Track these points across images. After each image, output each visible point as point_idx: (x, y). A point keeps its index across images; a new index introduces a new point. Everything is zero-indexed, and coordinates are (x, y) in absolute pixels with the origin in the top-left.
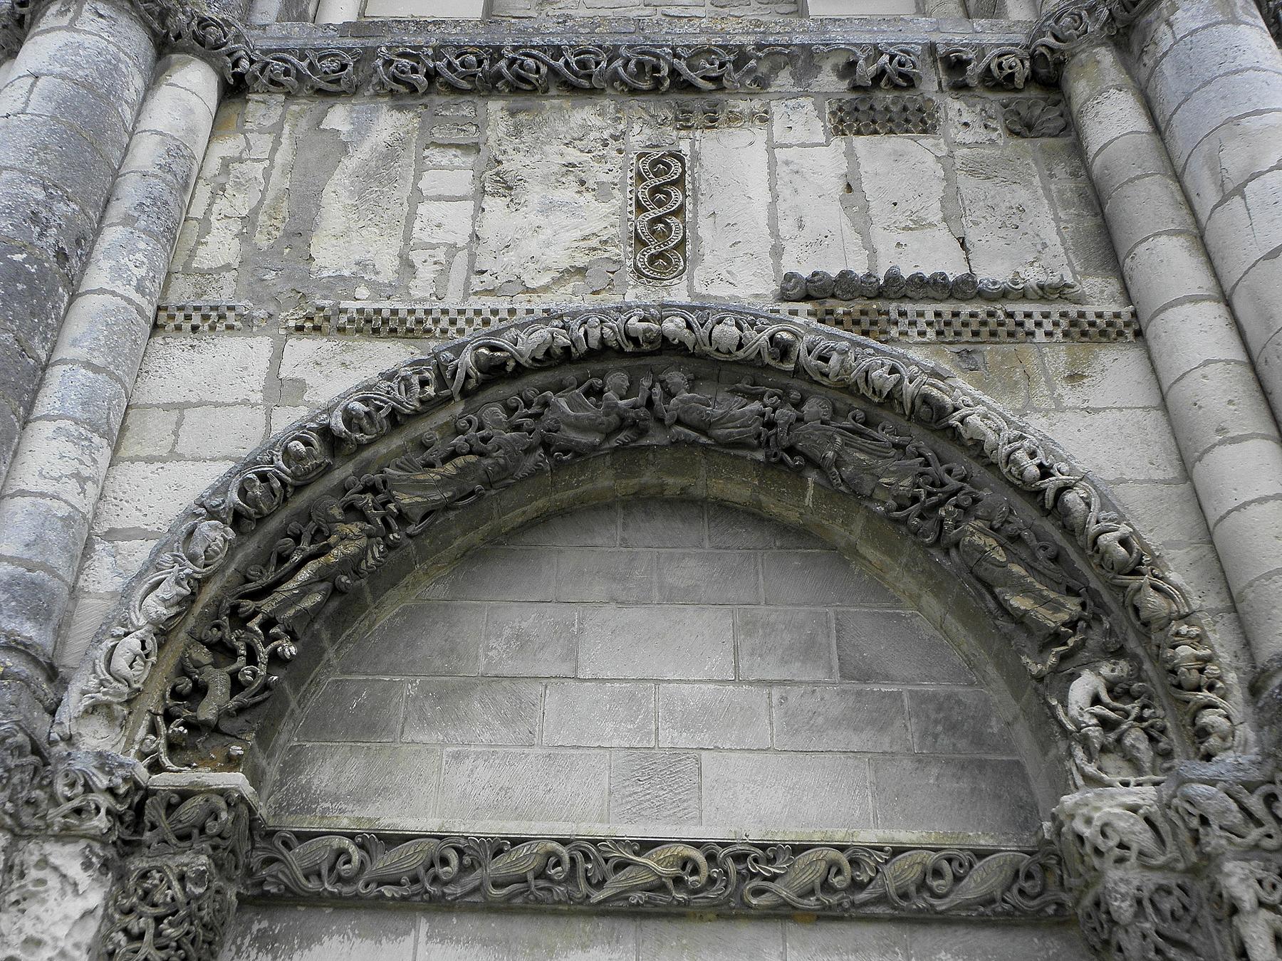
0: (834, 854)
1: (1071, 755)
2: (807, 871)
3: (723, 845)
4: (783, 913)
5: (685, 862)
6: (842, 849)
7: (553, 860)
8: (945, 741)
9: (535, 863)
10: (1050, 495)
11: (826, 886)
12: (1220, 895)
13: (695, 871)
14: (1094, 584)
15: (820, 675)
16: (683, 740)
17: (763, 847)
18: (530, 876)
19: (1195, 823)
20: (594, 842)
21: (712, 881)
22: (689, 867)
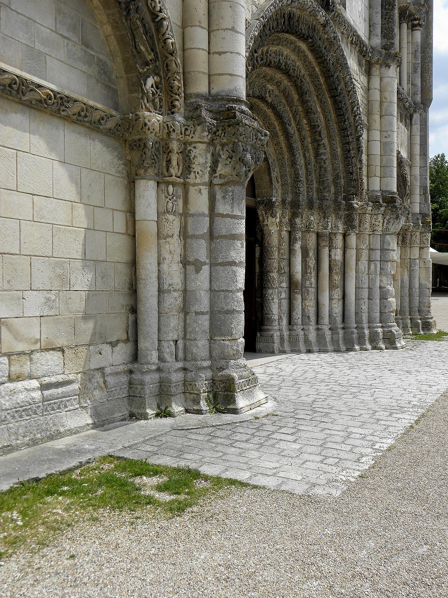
0: (83, 105)
1: (142, 98)
2: (76, 109)
3: (59, 93)
4: (67, 119)
5: (48, 95)
6: (85, 104)
7: (14, 82)
8: (103, 76)
9: (8, 82)
10: (159, 18)
11: (79, 114)
12: (169, 147)
13: (50, 99)
14: (158, 50)
15: (76, 40)
16: (42, 49)
17: (67, 97)
18: (7, 85)
19: (171, 130)
20: (26, 80)
21: (54, 103)
22: (49, 97)
